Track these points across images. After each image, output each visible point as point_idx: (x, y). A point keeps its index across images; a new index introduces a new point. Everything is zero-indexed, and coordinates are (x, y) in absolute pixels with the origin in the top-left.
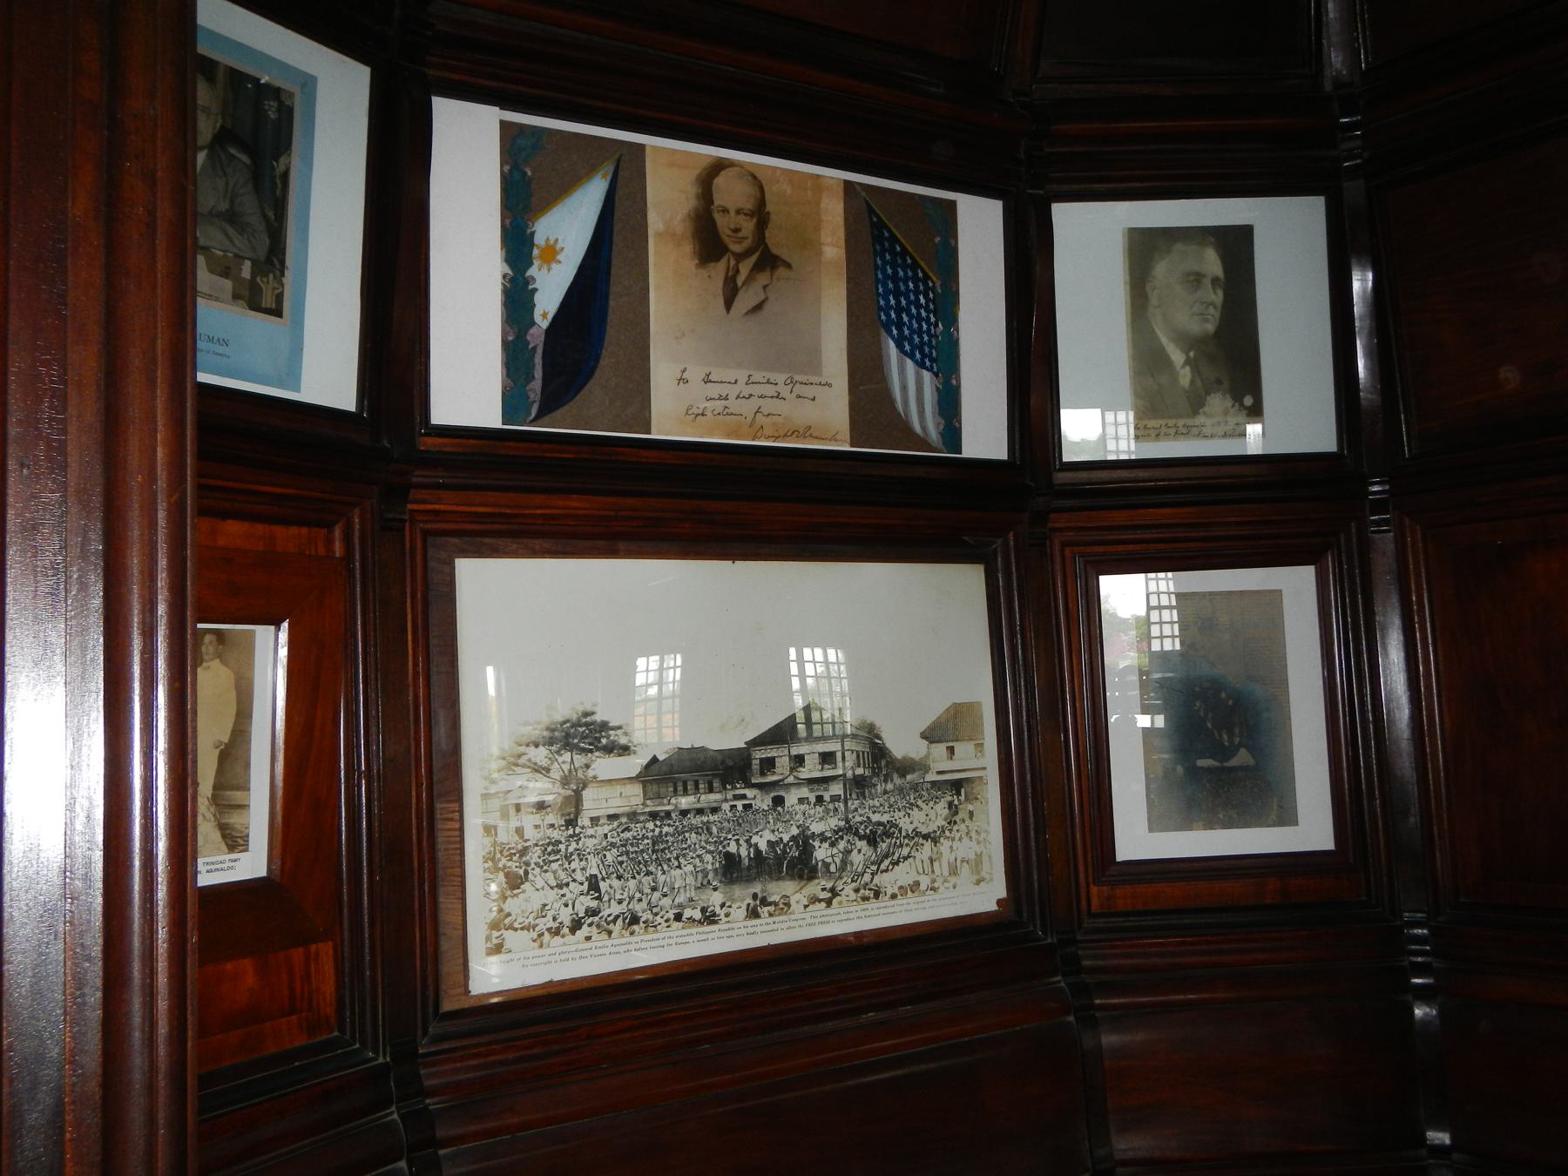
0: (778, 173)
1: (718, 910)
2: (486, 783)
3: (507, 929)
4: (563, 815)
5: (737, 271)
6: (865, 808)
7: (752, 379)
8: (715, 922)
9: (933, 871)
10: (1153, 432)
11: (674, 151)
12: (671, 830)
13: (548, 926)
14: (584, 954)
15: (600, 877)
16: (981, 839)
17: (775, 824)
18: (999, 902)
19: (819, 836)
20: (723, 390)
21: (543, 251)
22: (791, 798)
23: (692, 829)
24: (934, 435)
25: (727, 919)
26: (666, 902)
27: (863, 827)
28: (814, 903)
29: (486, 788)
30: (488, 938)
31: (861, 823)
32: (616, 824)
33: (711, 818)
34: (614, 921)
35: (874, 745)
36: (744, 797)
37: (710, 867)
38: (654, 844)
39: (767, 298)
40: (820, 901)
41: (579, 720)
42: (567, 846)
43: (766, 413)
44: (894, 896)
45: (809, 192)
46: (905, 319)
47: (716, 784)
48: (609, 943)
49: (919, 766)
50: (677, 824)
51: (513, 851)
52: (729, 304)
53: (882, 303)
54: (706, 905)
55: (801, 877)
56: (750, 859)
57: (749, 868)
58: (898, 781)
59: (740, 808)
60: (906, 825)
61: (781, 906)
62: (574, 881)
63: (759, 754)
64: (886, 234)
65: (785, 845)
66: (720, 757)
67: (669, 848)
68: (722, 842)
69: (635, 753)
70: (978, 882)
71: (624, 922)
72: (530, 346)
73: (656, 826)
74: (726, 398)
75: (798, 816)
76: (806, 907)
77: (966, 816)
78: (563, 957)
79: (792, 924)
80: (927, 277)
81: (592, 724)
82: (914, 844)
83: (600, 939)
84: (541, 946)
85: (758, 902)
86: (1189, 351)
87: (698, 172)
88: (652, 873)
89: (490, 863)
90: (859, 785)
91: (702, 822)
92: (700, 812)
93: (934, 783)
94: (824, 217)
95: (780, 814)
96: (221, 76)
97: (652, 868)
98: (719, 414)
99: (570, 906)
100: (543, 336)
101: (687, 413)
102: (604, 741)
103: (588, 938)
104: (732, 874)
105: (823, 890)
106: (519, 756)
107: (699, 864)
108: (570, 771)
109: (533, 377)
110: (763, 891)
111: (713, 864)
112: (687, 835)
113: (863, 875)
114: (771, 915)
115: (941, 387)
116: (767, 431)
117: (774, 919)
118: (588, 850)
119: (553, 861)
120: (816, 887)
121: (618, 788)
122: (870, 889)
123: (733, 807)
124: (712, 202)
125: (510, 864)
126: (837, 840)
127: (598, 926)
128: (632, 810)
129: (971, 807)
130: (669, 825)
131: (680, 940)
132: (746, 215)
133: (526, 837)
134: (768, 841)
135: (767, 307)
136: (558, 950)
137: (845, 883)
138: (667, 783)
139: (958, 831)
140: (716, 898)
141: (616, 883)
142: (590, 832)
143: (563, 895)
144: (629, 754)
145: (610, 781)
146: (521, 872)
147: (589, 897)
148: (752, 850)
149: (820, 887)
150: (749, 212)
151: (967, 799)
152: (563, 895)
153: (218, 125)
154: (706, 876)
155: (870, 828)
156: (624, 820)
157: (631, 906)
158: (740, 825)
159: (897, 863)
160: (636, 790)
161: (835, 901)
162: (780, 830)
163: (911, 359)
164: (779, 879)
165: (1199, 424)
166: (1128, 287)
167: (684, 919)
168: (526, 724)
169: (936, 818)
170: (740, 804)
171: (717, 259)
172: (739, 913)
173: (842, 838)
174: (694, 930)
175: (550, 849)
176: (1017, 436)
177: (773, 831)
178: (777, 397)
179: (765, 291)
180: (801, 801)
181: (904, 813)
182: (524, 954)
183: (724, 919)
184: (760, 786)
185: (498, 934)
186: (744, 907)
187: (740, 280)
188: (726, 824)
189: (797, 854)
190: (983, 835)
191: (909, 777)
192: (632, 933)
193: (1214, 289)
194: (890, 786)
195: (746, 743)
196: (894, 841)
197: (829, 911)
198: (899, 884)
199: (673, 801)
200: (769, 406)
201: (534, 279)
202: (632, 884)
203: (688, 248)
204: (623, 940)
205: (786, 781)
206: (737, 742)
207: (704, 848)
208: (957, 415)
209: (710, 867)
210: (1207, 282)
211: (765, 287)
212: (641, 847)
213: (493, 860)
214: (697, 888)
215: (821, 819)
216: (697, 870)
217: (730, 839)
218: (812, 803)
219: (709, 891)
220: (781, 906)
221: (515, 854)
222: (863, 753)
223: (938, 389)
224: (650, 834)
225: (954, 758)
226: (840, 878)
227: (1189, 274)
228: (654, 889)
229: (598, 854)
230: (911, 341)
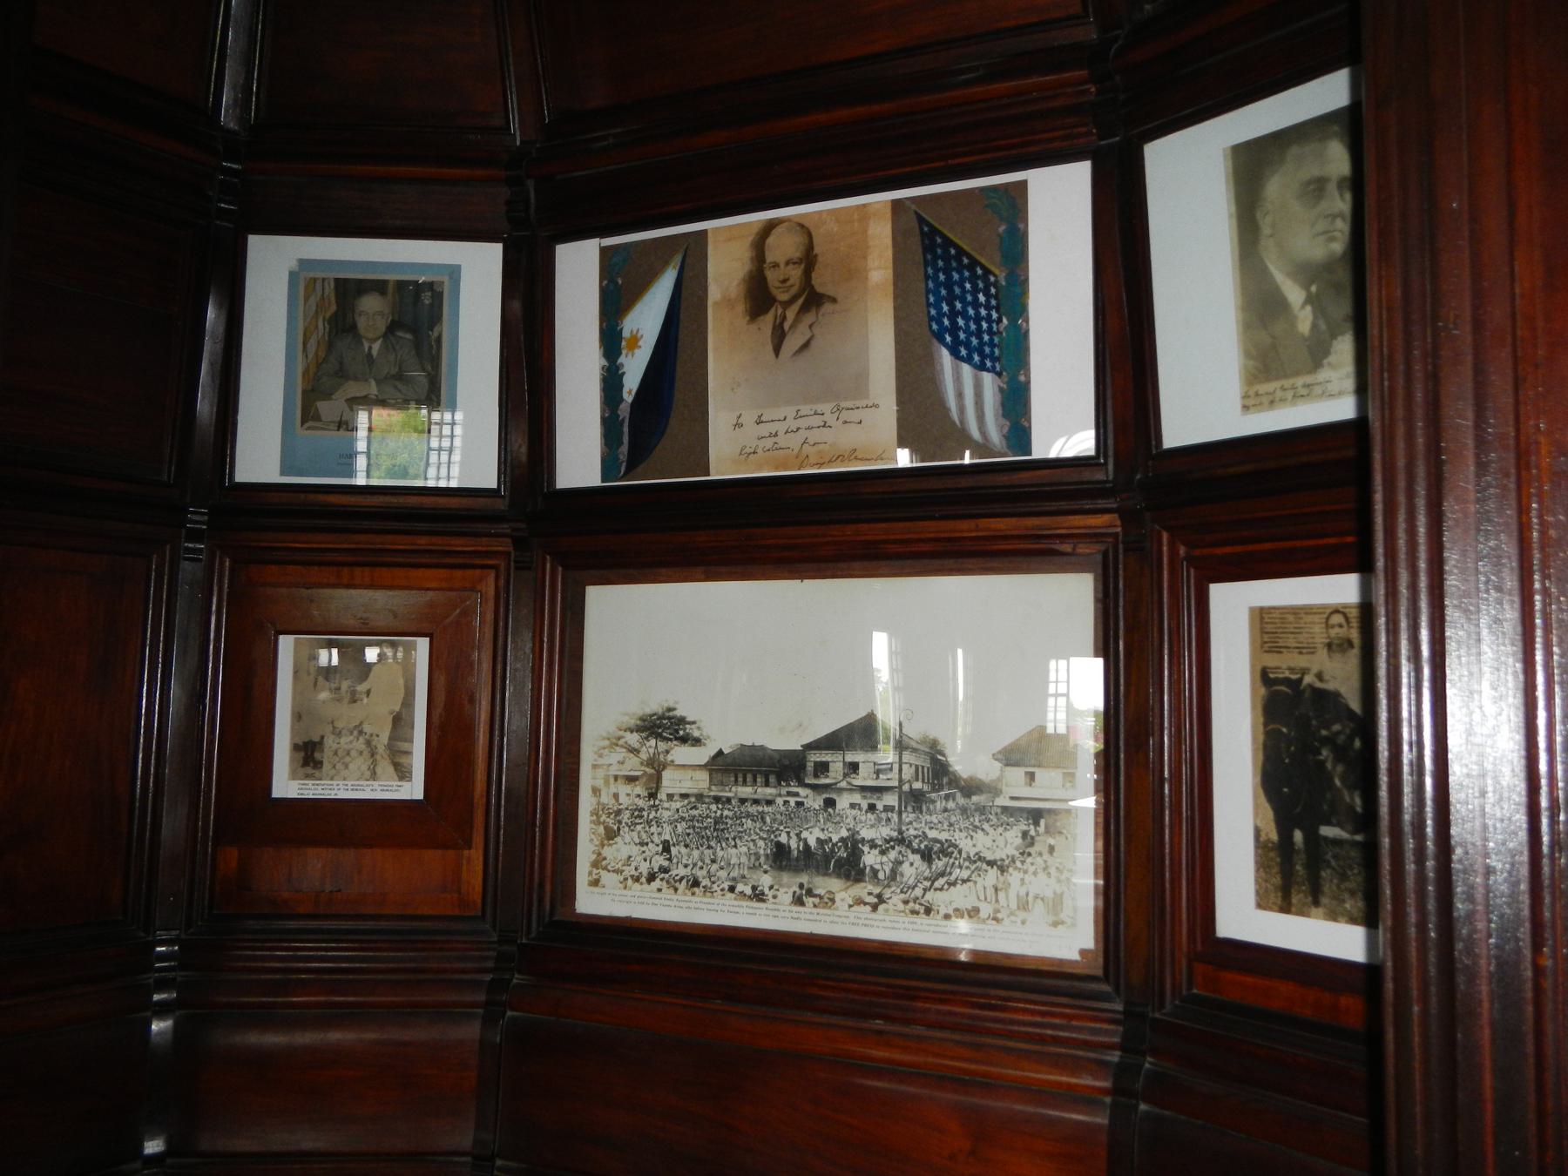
0: (824, 216)
1: (766, 891)
2: (596, 757)
3: (603, 869)
4: (647, 789)
5: (784, 318)
6: (921, 822)
7: (800, 413)
8: (763, 901)
9: (997, 901)
10: (1265, 400)
11: (730, 227)
12: (730, 814)
13: (632, 873)
14: (657, 902)
15: (671, 842)
16: (1063, 877)
17: (825, 824)
18: (1083, 952)
19: (868, 842)
20: (772, 428)
21: (628, 341)
22: (843, 802)
23: (748, 815)
24: (995, 437)
25: (774, 901)
26: (723, 874)
27: (917, 841)
28: (859, 904)
29: (595, 760)
30: (590, 873)
31: (916, 837)
32: (686, 801)
33: (766, 809)
34: (681, 880)
35: (934, 761)
36: (797, 794)
37: (762, 852)
38: (716, 823)
39: (813, 336)
40: (865, 904)
41: (663, 714)
42: (649, 814)
43: (812, 443)
44: (947, 917)
45: (856, 224)
46: (961, 322)
47: (772, 779)
48: (675, 897)
49: (993, 790)
50: (736, 809)
51: (611, 811)
52: (777, 350)
53: (933, 312)
54: (756, 884)
55: (847, 877)
56: (799, 851)
57: (797, 859)
58: (961, 800)
59: (792, 804)
60: (966, 845)
61: (826, 900)
62: (652, 842)
63: (815, 757)
64: (939, 240)
65: (834, 845)
66: (777, 756)
67: (728, 829)
68: (774, 832)
69: (705, 745)
70: (1055, 924)
71: (687, 883)
72: (621, 418)
73: (718, 808)
74: (776, 435)
75: (848, 820)
76: (850, 906)
77: (1045, 851)
78: (641, 900)
79: (836, 919)
80: (987, 272)
81: (673, 718)
82: (976, 869)
83: (668, 893)
84: (625, 888)
85: (804, 892)
86: (1310, 285)
87: (750, 239)
88: (712, 848)
89: (595, 818)
90: (916, 799)
91: (758, 811)
92: (756, 802)
93: (1005, 809)
94: (871, 243)
95: (830, 815)
96: (390, 288)
97: (713, 843)
98: (769, 450)
99: (648, 861)
100: (629, 410)
101: (741, 454)
102: (681, 733)
103: (660, 890)
104: (781, 862)
105: (870, 894)
106: (619, 738)
107: (752, 847)
108: (654, 754)
109: (623, 443)
110: (809, 883)
111: (765, 849)
112: (744, 820)
113: (913, 888)
114: (815, 906)
115: (1005, 386)
116: (812, 460)
117: (818, 910)
118: (664, 820)
119: (638, 824)
120: (865, 890)
121: (690, 773)
122: (921, 904)
123: (786, 802)
124: (764, 262)
125: (608, 820)
126: (887, 849)
127: (668, 882)
128: (700, 792)
129: (1051, 841)
130: (729, 809)
131: (732, 909)
132: (794, 263)
133: (620, 802)
134: (818, 839)
135: (813, 343)
136: (638, 894)
137: (893, 892)
138: (730, 773)
139: (1032, 864)
140: (765, 881)
141: (684, 850)
142: (666, 805)
143: (644, 852)
144: (700, 746)
145: (684, 766)
146: (616, 828)
147: (662, 857)
148: (801, 844)
149: (866, 891)
150: (798, 261)
151: (1047, 831)
152: (644, 852)
153: (389, 321)
154: (758, 859)
155: (926, 843)
156: (693, 800)
157: (694, 872)
158: (791, 819)
159: (953, 884)
160: (704, 776)
161: (881, 907)
162: (830, 829)
163: (970, 364)
164: (826, 874)
165: (1322, 380)
166: (1234, 221)
167: (736, 891)
168: (627, 714)
169: (1006, 846)
170: (792, 801)
171: (766, 311)
172: (785, 897)
173: (893, 848)
174: (745, 903)
175: (636, 813)
176: (1152, 422)
177: (823, 830)
178: (824, 426)
179: (811, 331)
180: (853, 806)
181: (966, 834)
182: (612, 891)
183: (771, 900)
184: (814, 787)
185: (598, 871)
186: (791, 894)
187: (786, 326)
188: (778, 816)
189: (845, 855)
190: (1066, 874)
191: (975, 799)
192: (693, 894)
193: (1341, 195)
194: (951, 805)
195: (802, 746)
196: (952, 860)
197: (873, 916)
198: (955, 905)
199: (734, 789)
200: (815, 436)
201: (622, 365)
202: (696, 853)
203: (741, 308)
204: (687, 898)
205: (838, 786)
206: (794, 744)
207: (758, 834)
208: (1026, 413)
209: (762, 852)
210: (1332, 187)
211: (810, 326)
212: (705, 824)
213: (597, 814)
214: (750, 868)
215: (872, 826)
216: (752, 852)
217: (782, 831)
218: (864, 809)
219: (760, 873)
220: (826, 900)
221: (612, 813)
222: (923, 767)
223: (1001, 390)
224: (713, 815)
225: (1033, 784)
226: (889, 886)
227: (1309, 183)
228: (713, 861)
229: (671, 824)
230: (967, 345)
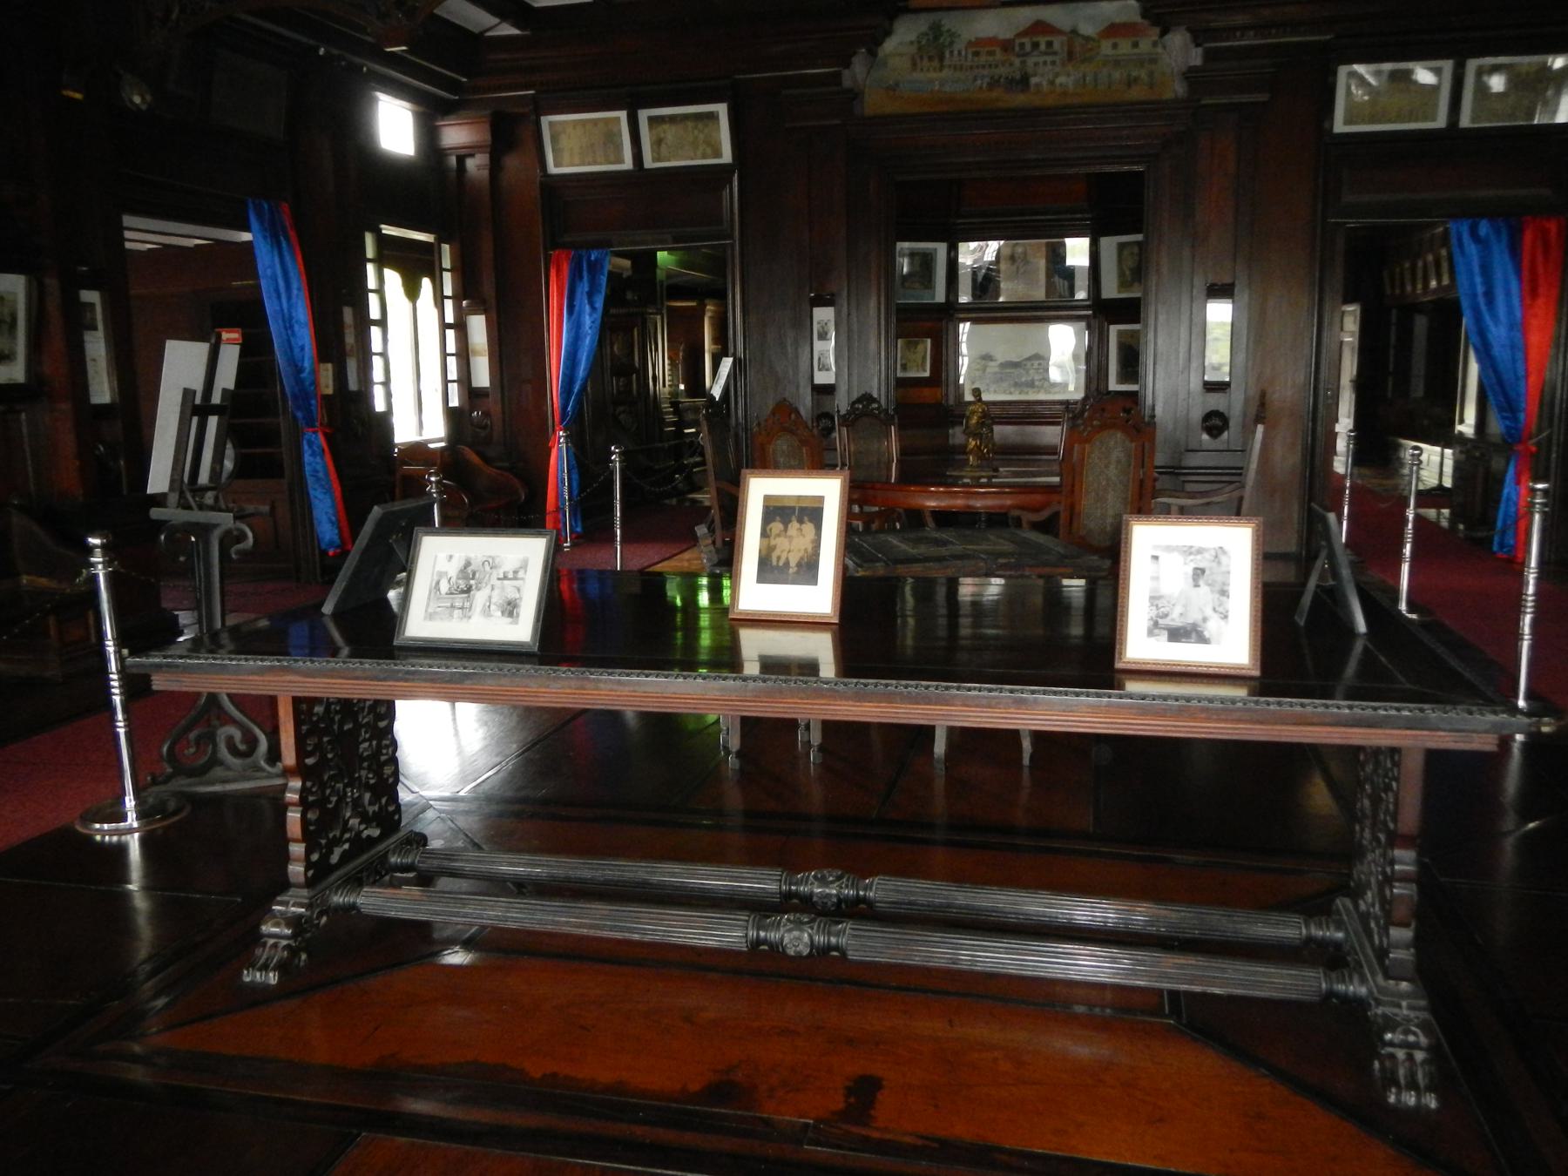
120: (1035, 390)
140: (1012, 390)
172: (1018, 392)
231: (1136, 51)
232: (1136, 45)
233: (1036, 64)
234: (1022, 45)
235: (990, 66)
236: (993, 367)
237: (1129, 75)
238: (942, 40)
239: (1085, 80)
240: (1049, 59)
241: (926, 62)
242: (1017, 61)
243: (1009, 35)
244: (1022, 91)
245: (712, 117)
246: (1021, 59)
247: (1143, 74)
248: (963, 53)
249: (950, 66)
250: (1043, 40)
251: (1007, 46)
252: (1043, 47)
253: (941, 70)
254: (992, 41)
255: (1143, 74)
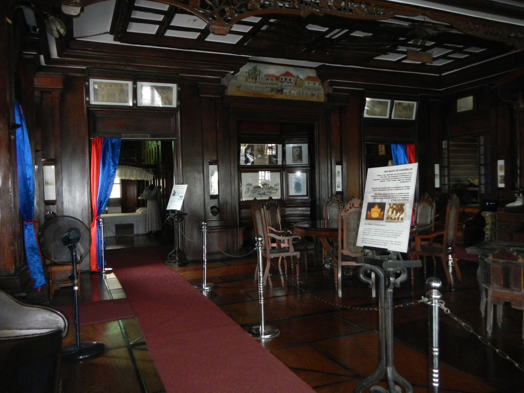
22: (264, 189)
24: (275, 163)
120: (266, 196)
140: (258, 196)
231: (314, 86)
232: (314, 84)
233: (285, 85)
234: (282, 79)
235: (272, 84)
236: (251, 188)
237: (312, 93)
238: (256, 73)
239: (300, 93)
240: (289, 84)
241: (251, 80)
242: (280, 84)
243: (278, 75)
244: (281, 94)
245: (170, 89)
246: (282, 83)
247: (316, 93)
248: (263, 78)
249: (258, 82)
250: (288, 78)
251: (277, 78)
252: (288, 80)
253: (255, 83)
254: (273, 76)
255: (316, 93)
